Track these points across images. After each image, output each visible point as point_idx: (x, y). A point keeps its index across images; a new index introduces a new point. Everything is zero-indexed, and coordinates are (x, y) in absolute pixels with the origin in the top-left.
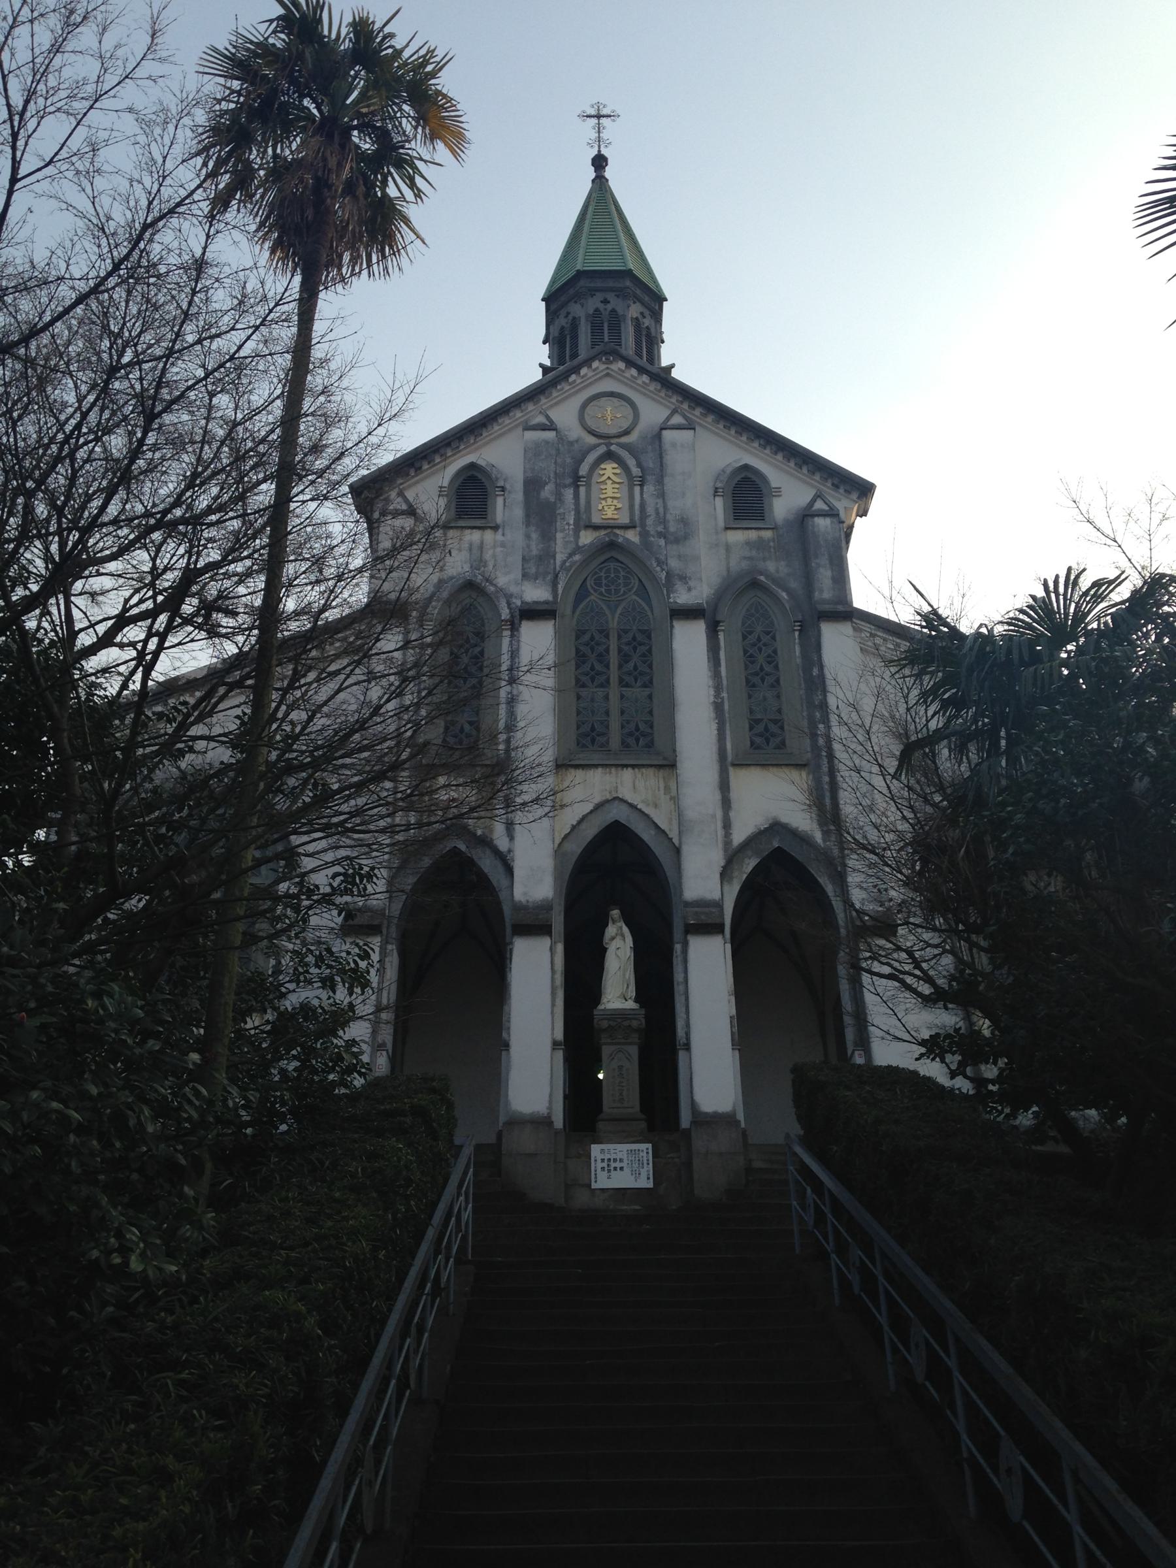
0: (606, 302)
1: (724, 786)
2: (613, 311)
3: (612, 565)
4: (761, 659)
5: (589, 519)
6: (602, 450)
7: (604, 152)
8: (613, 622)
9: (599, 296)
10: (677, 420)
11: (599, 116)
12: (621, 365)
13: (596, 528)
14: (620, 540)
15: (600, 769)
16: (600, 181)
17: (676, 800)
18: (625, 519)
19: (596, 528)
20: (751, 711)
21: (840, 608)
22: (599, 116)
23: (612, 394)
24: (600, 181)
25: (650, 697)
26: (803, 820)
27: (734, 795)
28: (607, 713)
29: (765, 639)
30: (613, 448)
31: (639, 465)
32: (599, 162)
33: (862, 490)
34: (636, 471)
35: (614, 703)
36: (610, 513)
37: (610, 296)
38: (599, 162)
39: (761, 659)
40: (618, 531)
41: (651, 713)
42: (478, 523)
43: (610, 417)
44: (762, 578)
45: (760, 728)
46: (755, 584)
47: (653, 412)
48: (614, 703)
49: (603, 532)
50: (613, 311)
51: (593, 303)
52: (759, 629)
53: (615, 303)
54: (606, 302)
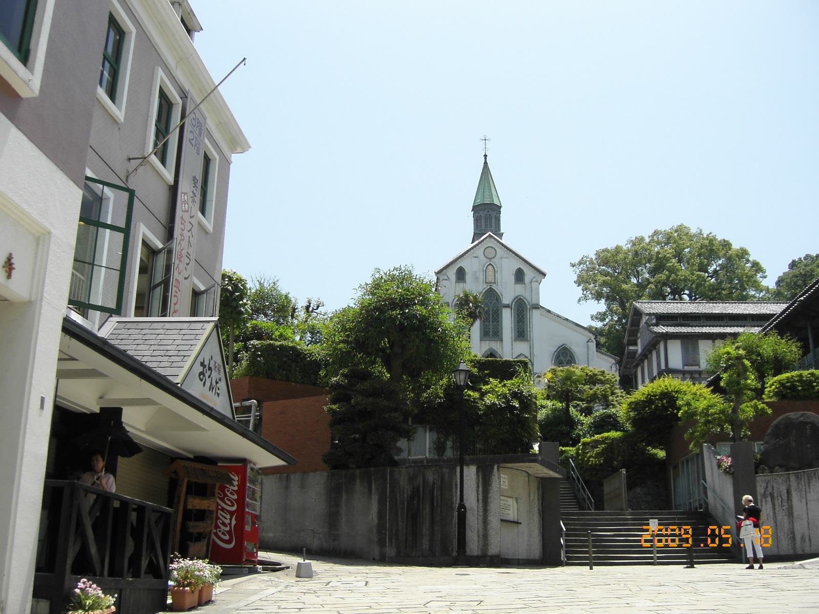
0: (488, 212)
1: (512, 345)
2: (490, 215)
3: (490, 293)
4: (520, 316)
5: (486, 280)
6: (489, 263)
7: (487, 154)
8: (491, 309)
9: (487, 211)
10: (505, 256)
11: (485, 140)
12: (493, 240)
13: (488, 283)
14: (493, 287)
15: (488, 341)
16: (486, 163)
17: (502, 348)
18: (494, 281)
19: (488, 283)
20: (518, 329)
21: (537, 306)
22: (485, 140)
23: (491, 247)
24: (486, 163)
25: (498, 325)
26: (527, 354)
27: (513, 347)
28: (490, 328)
29: (522, 311)
30: (491, 263)
31: (497, 267)
32: (485, 156)
33: (544, 275)
34: (496, 270)
35: (491, 326)
36: (490, 279)
37: (490, 211)
38: (485, 156)
39: (520, 316)
40: (492, 285)
41: (498, 329)
42: (463, 281)
43: (490, 253)
44: (522, 297)
45: (520, 332)
46: (520, 298)
47: (500, 251)
48: (491, 326)
49: (489, 284)
50: (490, 215)
51: (486, 212)
52: (520, 309)
53: (491, 212)
54: (488, 212)
